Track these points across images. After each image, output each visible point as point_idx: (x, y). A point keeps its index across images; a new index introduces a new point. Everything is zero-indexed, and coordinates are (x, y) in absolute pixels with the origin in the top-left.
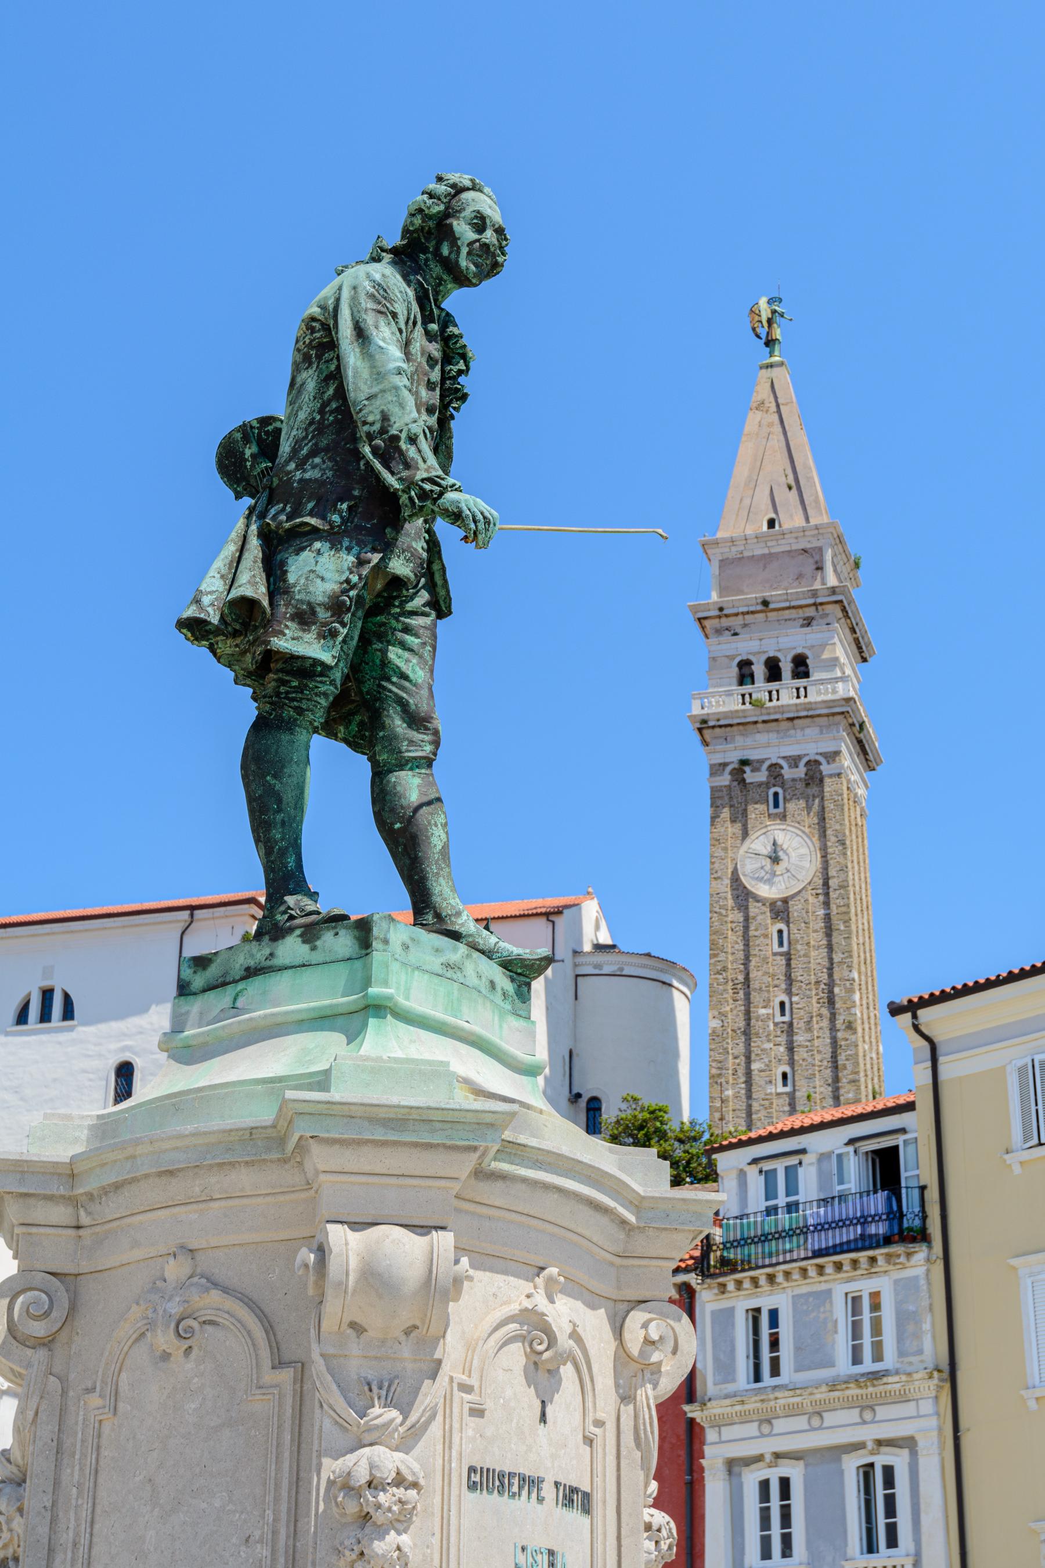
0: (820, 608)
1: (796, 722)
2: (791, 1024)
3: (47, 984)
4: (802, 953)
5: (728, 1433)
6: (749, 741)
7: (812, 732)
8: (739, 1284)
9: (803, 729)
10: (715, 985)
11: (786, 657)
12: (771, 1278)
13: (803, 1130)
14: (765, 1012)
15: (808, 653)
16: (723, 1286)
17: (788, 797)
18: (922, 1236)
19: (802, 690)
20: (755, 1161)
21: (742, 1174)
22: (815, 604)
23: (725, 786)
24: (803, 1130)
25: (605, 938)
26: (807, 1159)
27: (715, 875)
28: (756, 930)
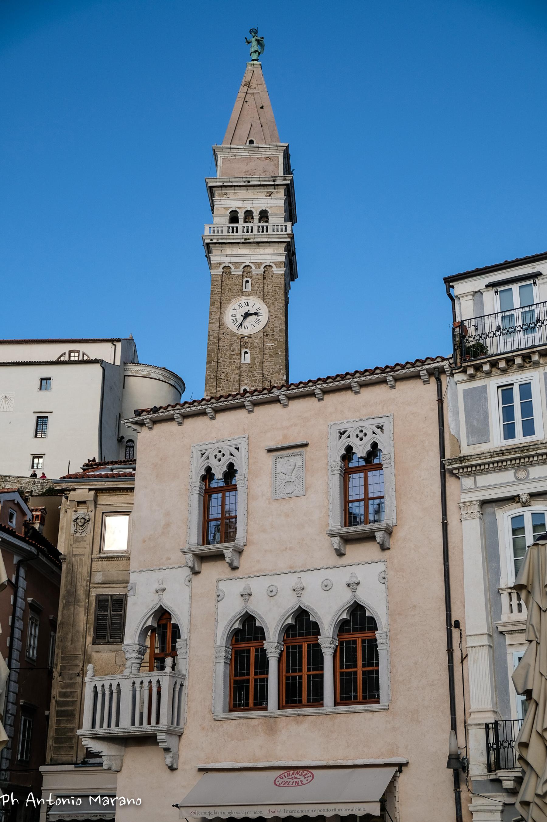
0: (276, 187)
1: (260, 244)
4: (257, 364)
5: (483, 480)
7: (269, 250)
8: (494, 364)
9: (264, 249)
10: (209, 379)
11: (256, 211)
16: (478, 368)
17: (254, 283)
19: (265, 228)
22: (274, 185)
23: (220, 275)
27: (212, 321)
28: (233, 351)
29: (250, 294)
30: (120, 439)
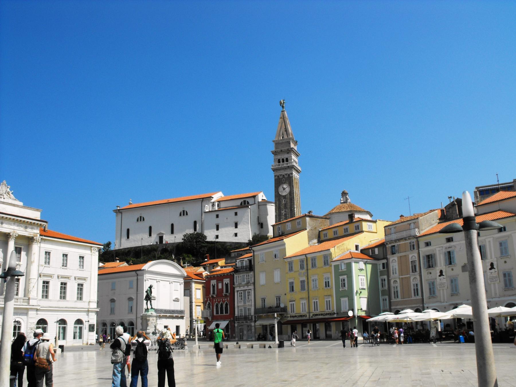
2: (286, 214)
3: (183, 210)
5: (237, 288)
6: (280, 172)
7: (289, 170)
8: (237, 274)
12: (240, 273)
13: (244, 258)
14: (283, 212)
15: (288, 158)
18: (252, 270)
20: (240, 261)
21: (239, 262)
24: (244, 258)
25: (264, 198)
26: (245, 261)
29: (285, 183)
30: (259, 223)
